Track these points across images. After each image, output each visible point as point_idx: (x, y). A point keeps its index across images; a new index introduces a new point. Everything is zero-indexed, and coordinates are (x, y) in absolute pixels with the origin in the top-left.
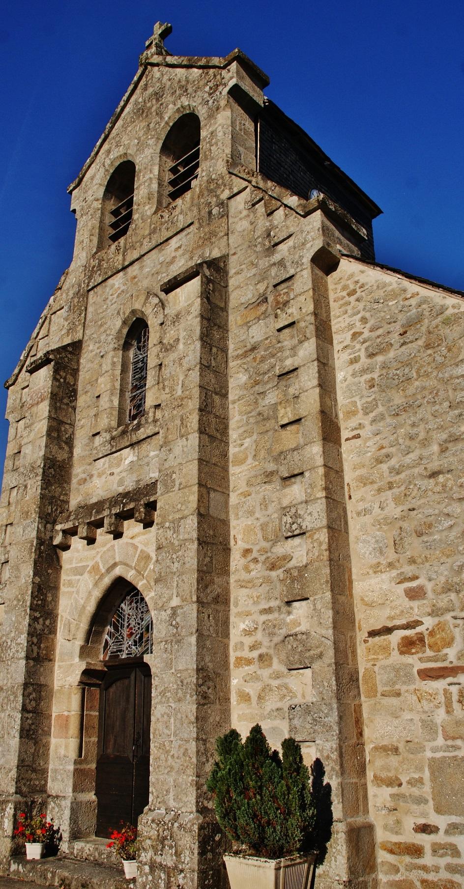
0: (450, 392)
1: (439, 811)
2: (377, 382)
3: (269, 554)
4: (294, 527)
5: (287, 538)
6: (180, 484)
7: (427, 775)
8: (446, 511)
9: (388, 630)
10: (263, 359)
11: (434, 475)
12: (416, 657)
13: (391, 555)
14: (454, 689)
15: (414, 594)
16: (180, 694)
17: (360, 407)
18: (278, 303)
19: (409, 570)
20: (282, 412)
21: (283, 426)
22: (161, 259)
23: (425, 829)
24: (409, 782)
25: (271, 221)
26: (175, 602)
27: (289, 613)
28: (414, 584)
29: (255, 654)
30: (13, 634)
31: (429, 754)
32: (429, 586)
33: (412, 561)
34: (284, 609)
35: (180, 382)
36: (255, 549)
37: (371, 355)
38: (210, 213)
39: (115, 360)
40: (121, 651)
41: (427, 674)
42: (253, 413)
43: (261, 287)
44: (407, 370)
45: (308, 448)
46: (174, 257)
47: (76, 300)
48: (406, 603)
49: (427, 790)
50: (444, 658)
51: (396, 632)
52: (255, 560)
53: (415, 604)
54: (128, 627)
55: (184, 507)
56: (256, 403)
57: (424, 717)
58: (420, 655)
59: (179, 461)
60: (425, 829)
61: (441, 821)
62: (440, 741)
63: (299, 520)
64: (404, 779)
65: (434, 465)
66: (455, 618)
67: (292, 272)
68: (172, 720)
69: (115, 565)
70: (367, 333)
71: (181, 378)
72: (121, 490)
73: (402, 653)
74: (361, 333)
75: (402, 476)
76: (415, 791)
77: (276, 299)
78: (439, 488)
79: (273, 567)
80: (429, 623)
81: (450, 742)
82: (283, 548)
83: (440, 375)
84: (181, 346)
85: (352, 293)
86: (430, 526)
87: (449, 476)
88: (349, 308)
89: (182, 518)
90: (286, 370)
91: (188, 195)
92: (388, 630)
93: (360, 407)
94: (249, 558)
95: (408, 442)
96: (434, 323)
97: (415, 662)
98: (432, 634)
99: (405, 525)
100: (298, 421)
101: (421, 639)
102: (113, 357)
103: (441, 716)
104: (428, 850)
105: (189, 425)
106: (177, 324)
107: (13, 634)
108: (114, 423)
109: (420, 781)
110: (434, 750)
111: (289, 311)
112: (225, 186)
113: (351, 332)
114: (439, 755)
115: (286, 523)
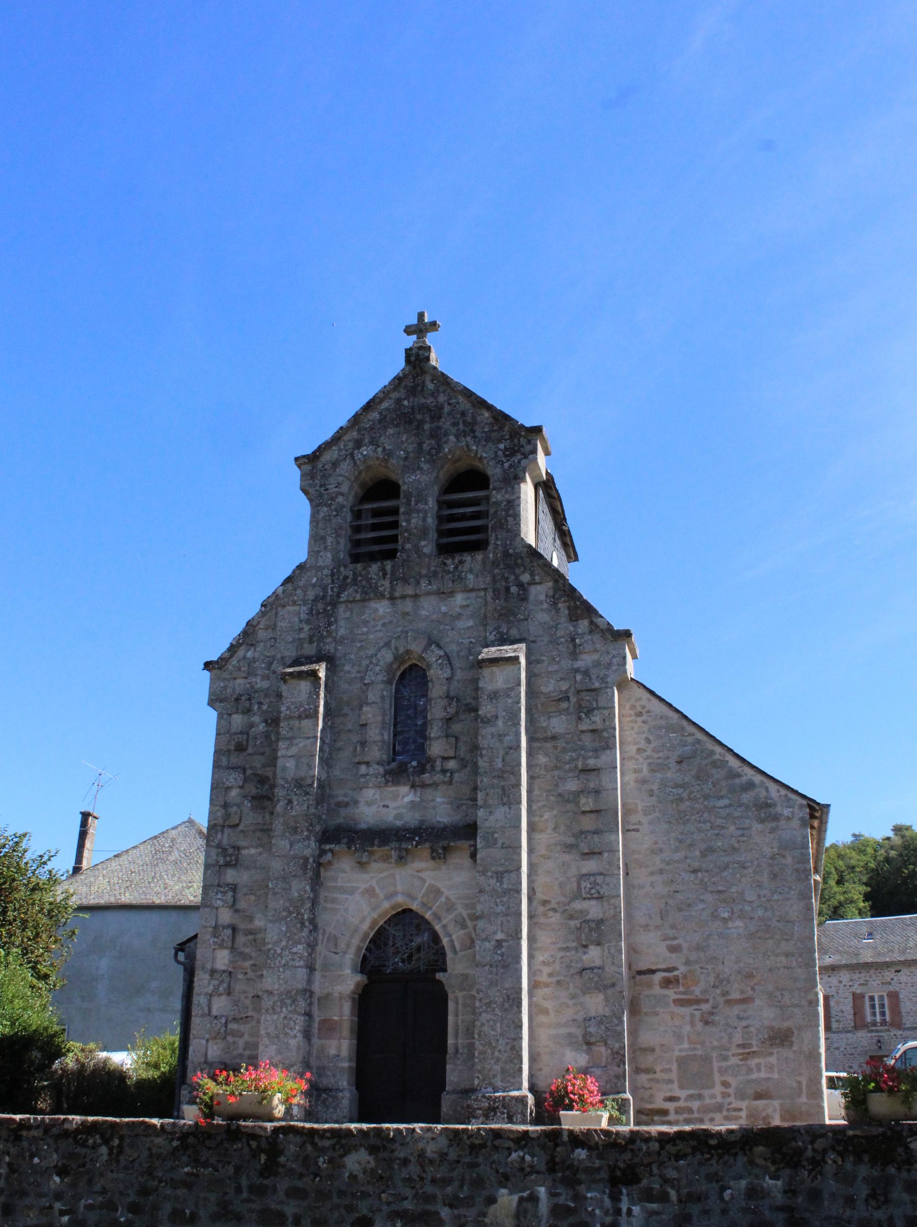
0: (713, 817)
1: (681, 1087)
2: (656, 792)
3: (567, 907)
4: (593, 891)
5: (585, 899)
6: (503, 844)
7: (674, 1067)
8: (702, 897)
9: (653, 972)
10: (564, 750)
11: (695, 871)
12: (672, 991)
13: (658, 921)
14: (697, 1013)
15: (674, 949)
16: (506, 1005)
17: (640, 808)
18: (580, 706)
19: (671, 933)
20: (583, 800)
21: (584, 812)
22: (444, 609)
23: (671, 1099)
24: (662, 1071)
25: (575, 627)
26: (500, 936)
27: (585, 953)
28: (675, 942)
29: (554, 980)
30: (284, 943)
31: (677, 1053)
32: (685, 946)
33: (673, 927)
34: (581, 950)
35: (500, 756)
36: (553, 901)
37: (653, 771)
38: (507, 589)
39: (385, 693)
40: (384, 966)
41: (680, 1003)
42: (554, 793)
43: (564, 686)
44: (681, 791)
45: (607, 834)
46: (460, 614)
47: (320, 606)
48: (668, 954)
49: (674, 1075)
50: (692, 993)
51: (658, 973)
52: (554, 910)
53: (673, 956)
54: (393, 945)
55: (507, 863)
56: (557, 785)
57: (676, 1030)
58: (675, 990)
59: (501, 824)
60: (671, 1099)
61: (682, 1094)
62: (686, 1045)
63: (598, 887)
64: (658, 1069)
65: (696, 865)
66: (702, 968)
67: (597, 685)
68: (498, 1025)
69: (395, 893)
70: (649, 752)
71: (502, 753)
72: (399, 823)
73: (662, 987)
74: (645, 751)
75: (670, 867)
76: (666, 1076)
77: (578, 701)
78: (698, 882)
79: (571, 918)
80: (682, 969)
81: (693, 1046)
82: (578, 905)
83: (706, 803)
84: (500, 723)
85: (640, 714)
86: (689, 905)
87: (706, 874)
88: (636, 726)
89: (507, 872)
90: (589, 768)
91: (479, 556)
92: (653, 972)
93: (640, 808)
94: (548, 907)
95: (677, 844)
96: (704, 762)
97: (671, 994)
98: (685, 977)
99: (670, 902)
100: (597, 811)
101: (677, 980)
102: (383, 690)
103: (687, 1028)
104: (672, 1111)
105: (511, 796)
106: (494, 701)
107: (284, 943)
108: (385, 757)
109: (670, 1070)
110: (681, 1050)
111: (594, 719)
112: (525, 569)
113: (636, 747)
114: (683, 1054)
115: (585, 887)
